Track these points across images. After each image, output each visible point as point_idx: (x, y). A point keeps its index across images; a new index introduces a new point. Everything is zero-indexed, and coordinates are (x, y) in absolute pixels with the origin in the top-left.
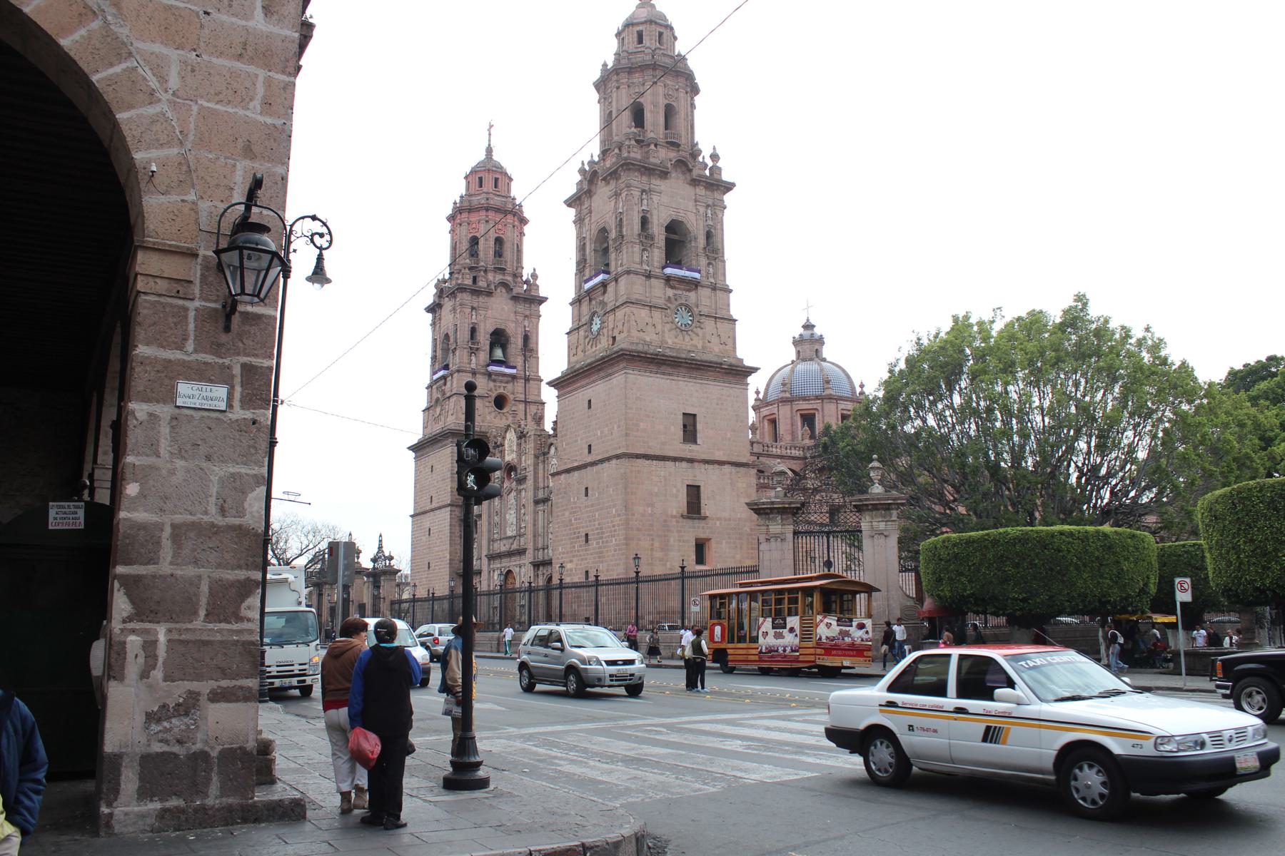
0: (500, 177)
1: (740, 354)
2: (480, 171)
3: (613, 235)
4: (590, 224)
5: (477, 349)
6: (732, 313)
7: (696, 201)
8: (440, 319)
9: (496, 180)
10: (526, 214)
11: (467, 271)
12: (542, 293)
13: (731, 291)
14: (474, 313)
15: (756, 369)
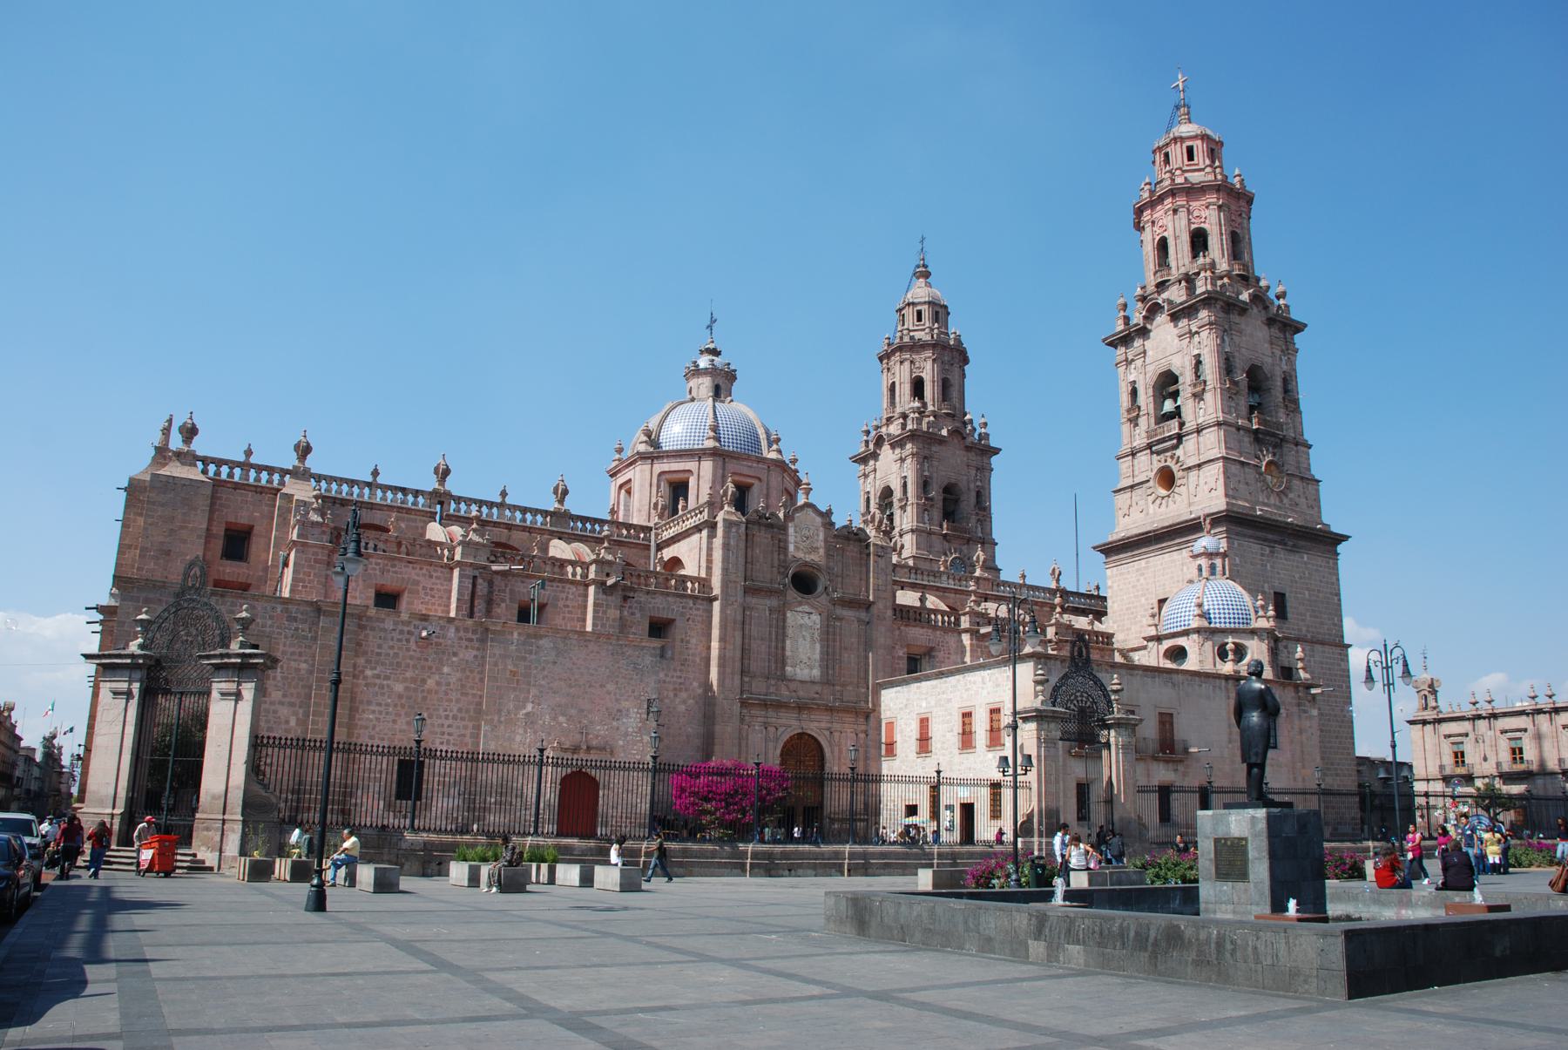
0: (940, 310)
1: (1325, 519)
2: (920, 303)
3: (1186, 379)
4: (1144, 365)
5: (932, 506)
6: (1313, 472)
7: (1272, 344)
8: (875, 470)
9: (937, 313)
10: (969, 354)
11: (917, 415)
12: (993, 443)
13: (1310, 447)
14: (926, 465)
15: (1344, 538)
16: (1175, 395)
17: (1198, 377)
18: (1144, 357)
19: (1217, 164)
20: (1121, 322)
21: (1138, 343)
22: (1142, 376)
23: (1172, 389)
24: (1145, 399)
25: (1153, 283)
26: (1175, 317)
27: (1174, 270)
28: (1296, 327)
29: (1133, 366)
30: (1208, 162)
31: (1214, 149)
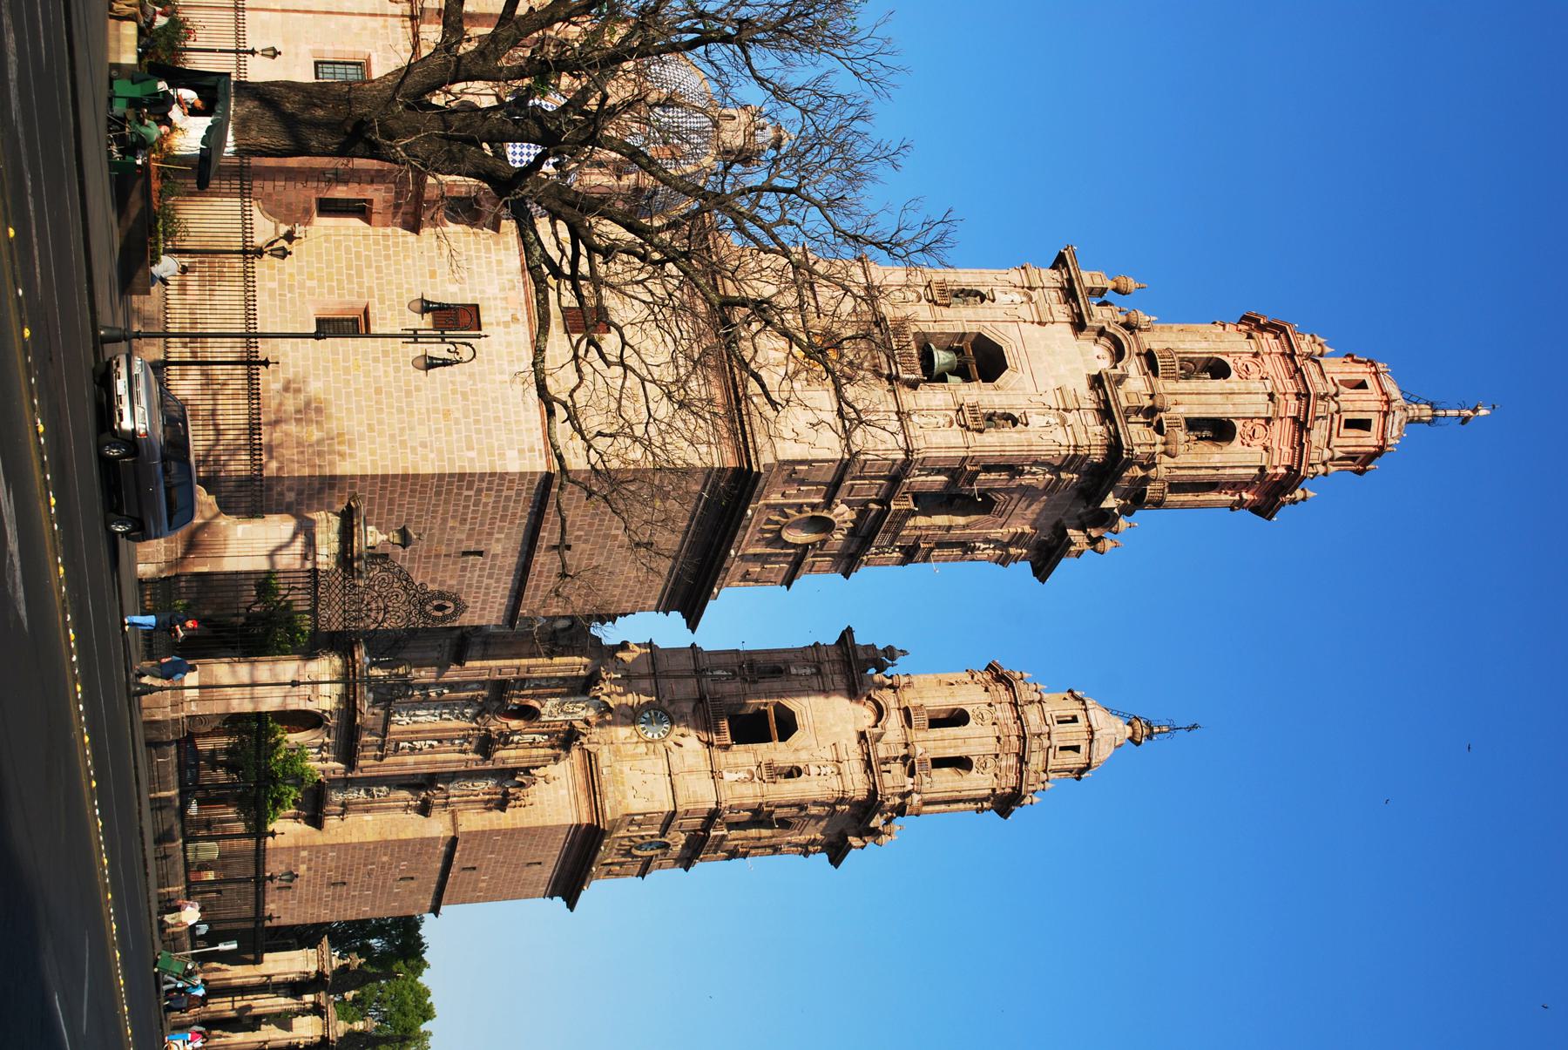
13: (846, 575)
16: (964, 374)
17: (990, 418)
18: (1033, 322)
19: (1332, 469)
20: (1098, 283)
21: (1061, 312)
22: (1000, 315)
23: (974, 371)
24: (961, 319)
25: (1155, 347)
26: (1097, 381)
27: (1171, 386)
28: (1043, 566)
29: (1017, 298)
30: (1338, 454)
31: (1361, 462)
